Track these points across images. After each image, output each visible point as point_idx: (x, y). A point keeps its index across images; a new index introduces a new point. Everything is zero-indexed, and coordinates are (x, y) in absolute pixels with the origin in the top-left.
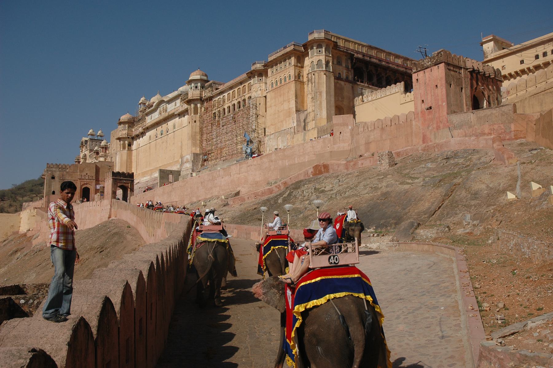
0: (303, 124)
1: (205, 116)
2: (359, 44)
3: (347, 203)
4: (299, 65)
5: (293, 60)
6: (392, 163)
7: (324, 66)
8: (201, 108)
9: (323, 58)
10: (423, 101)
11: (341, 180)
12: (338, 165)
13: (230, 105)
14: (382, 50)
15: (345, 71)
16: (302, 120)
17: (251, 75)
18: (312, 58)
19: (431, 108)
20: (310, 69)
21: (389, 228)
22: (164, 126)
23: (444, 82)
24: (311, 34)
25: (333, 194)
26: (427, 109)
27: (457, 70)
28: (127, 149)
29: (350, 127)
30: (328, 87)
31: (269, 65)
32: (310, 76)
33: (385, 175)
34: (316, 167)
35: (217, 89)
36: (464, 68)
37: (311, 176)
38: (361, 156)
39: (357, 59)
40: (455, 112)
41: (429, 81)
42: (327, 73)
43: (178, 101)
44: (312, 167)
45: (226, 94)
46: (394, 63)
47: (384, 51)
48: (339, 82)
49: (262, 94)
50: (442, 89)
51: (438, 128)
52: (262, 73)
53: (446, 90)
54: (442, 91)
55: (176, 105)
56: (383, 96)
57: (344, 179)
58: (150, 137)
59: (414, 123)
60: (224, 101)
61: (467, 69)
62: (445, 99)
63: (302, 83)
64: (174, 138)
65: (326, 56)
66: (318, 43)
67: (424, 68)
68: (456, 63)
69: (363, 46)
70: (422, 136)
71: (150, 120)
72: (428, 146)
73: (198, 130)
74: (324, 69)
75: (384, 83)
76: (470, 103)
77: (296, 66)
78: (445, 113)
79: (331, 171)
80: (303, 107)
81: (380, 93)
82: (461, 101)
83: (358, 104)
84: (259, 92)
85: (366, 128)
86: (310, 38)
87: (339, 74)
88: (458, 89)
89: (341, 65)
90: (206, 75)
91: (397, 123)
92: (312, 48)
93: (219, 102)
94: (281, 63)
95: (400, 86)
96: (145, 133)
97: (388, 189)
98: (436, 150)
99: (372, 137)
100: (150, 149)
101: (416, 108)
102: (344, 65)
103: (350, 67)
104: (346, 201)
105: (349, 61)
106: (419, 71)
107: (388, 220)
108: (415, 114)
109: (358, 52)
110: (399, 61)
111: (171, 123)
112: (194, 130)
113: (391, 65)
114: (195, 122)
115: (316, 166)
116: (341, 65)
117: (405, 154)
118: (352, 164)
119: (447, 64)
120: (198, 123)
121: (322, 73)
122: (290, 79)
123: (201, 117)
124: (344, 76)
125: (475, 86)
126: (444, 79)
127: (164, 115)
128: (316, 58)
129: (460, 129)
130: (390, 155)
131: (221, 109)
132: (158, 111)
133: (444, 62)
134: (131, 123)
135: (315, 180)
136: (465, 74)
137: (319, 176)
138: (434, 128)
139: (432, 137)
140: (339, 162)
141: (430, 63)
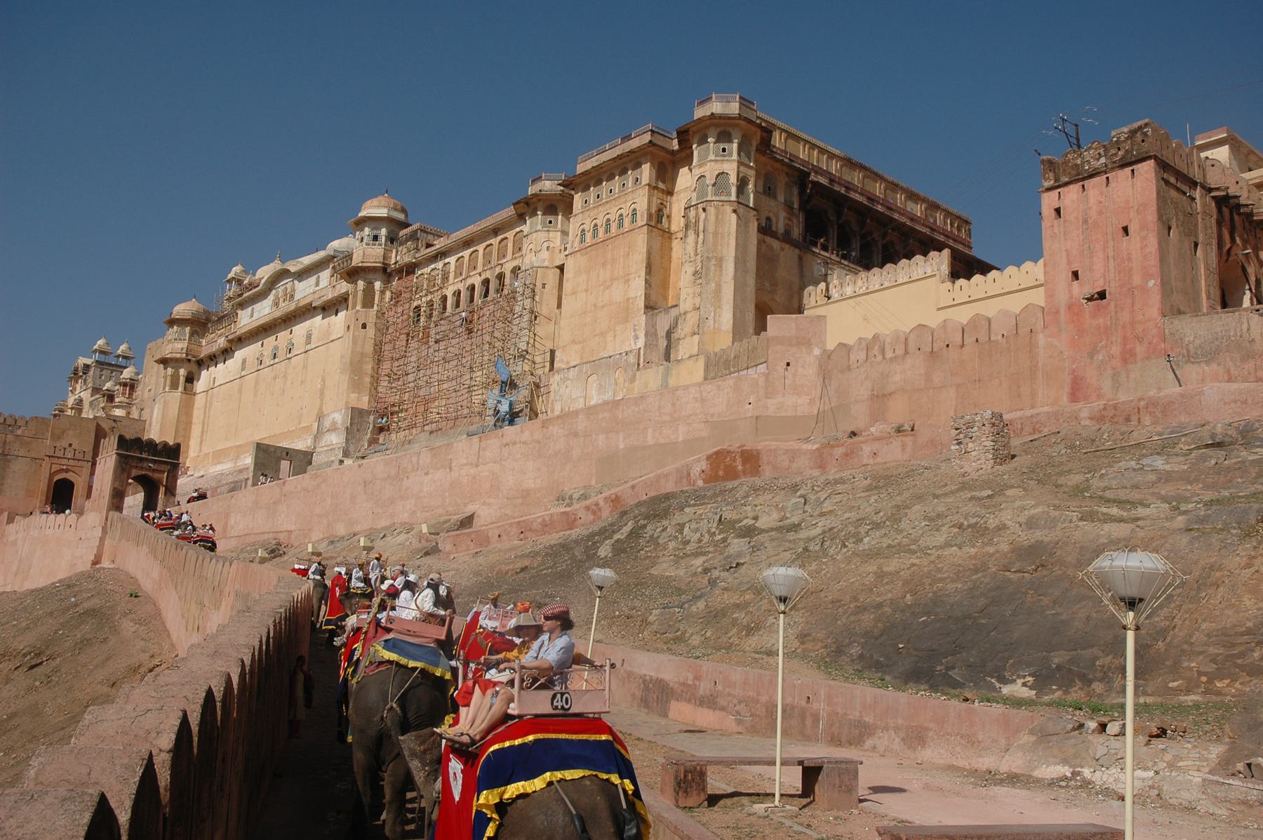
0: (663, 343)
1: (392, 313)
2: (822, 151)
3: (880, 575)
4: (661, 185)
6: (1004, 456)
7: (734, 190)
8: (383, 292)
10: (1075, 275)
11: (812, 497)
12: (793, 455)
13: (461, 286)
14: (877, 174)
15: (783, 215)
16: (662, 333)
17: (527, 207)
18: (700, 166)
19: (1102, 295)
20: (694, 195)
21: (1098, 687)
22: (283, 335)
23: (1151, 216)
24: (701, 103)
25: (809, 540)
26: (1090, 299)
27: (1185, 188)
28: (181, 389)
29: (817, 352)
30: (741, 247)
32: (692, 213)
33: (1000, 489)
34: (717, 458)
35: (429, 246)
36: (1203, 187)
37: (700, 483)
38: (853, 434)
39: (816, 184)
40: (1180, 312)
41: (1100, 213)
42: (741, 210)
43: (325, 275)
44: (703, 455)
45: (452, 260)
46: (903, 212)
47: (882, 178)
48: (768, 239)
49: (552, 259)
50: (1145, 238)
51: (1128, 357)
52: (557, 206)
53: (1160, 243)
54: (1144, 245)
55: (317, 284)
56: (886, 284)
57: (823, 495)
58: (244, 361)
59: (1041, 339)
60: (445, 278)
61: (1210, 190)
62: (1155, 270)
63: (668, 235)
64: (305, 367)
65: (740, 163)
66: (722, 128)
67: (1082, 177)
68: (1181, 166)
69: (832, 156)
70: (1067, 379)
71: (247, 319)
72: (1115, 407)
73: (369, 348)
74: (733, 198)
75: (877, 257)
76: (1216, 293)
78: (1154, 311)
79: (767, 472)
80: (666, 298)
81: (877, 277)
82: (1195, 281)
83: (813, 303)
84: (545, 254)
85: (876, 350)
86: (700, 113)
87: (768, 219)
88: (1188, 245)
89: (775, 197)
90: (403, 211)
91: (983, 338)
92: (703, 141)
93: (431, 280)
94: (611, 177)
95: (940, 262)
96: (233, 352)
97: (1038, 535)
98: (1147, 420)
99: (897, 378)
100: (240, 391)
101: (1050, 296)
102: (781, 198)
103: (796, 206)
104: (872, 568)
105: (795, 191)
106: (1066, 184)
107: (1088, 653)
108: (1049, 313)
109: (819, 171)
110: (918, 209)
111: (300, 329)
112: (359, 349)
113: (896, 216)
115: (717, 453)
116: (775, 197)
117: (1028, 429)
118: (838, 452)
119: (1163, 166)
120: (371, 331)
121: (728, 209)
122: (633, 221)
123: (380, 314)
124: (780, 227)
125: (1228, 246)
126: (1154, 208)
127: (286, 307)
128: (716, 164)
129: (1208, 363)
130: (999, 426)
131: (436, 298)
132: (271, 297)
133: (1155, 158)
134: (200, 324)
135: (715, 496)
136: (1204, 205)
137: (730, 485)
138: (1111, 357)
139: (1107, 385)
140: (795, 445)
141: (1103, 160)
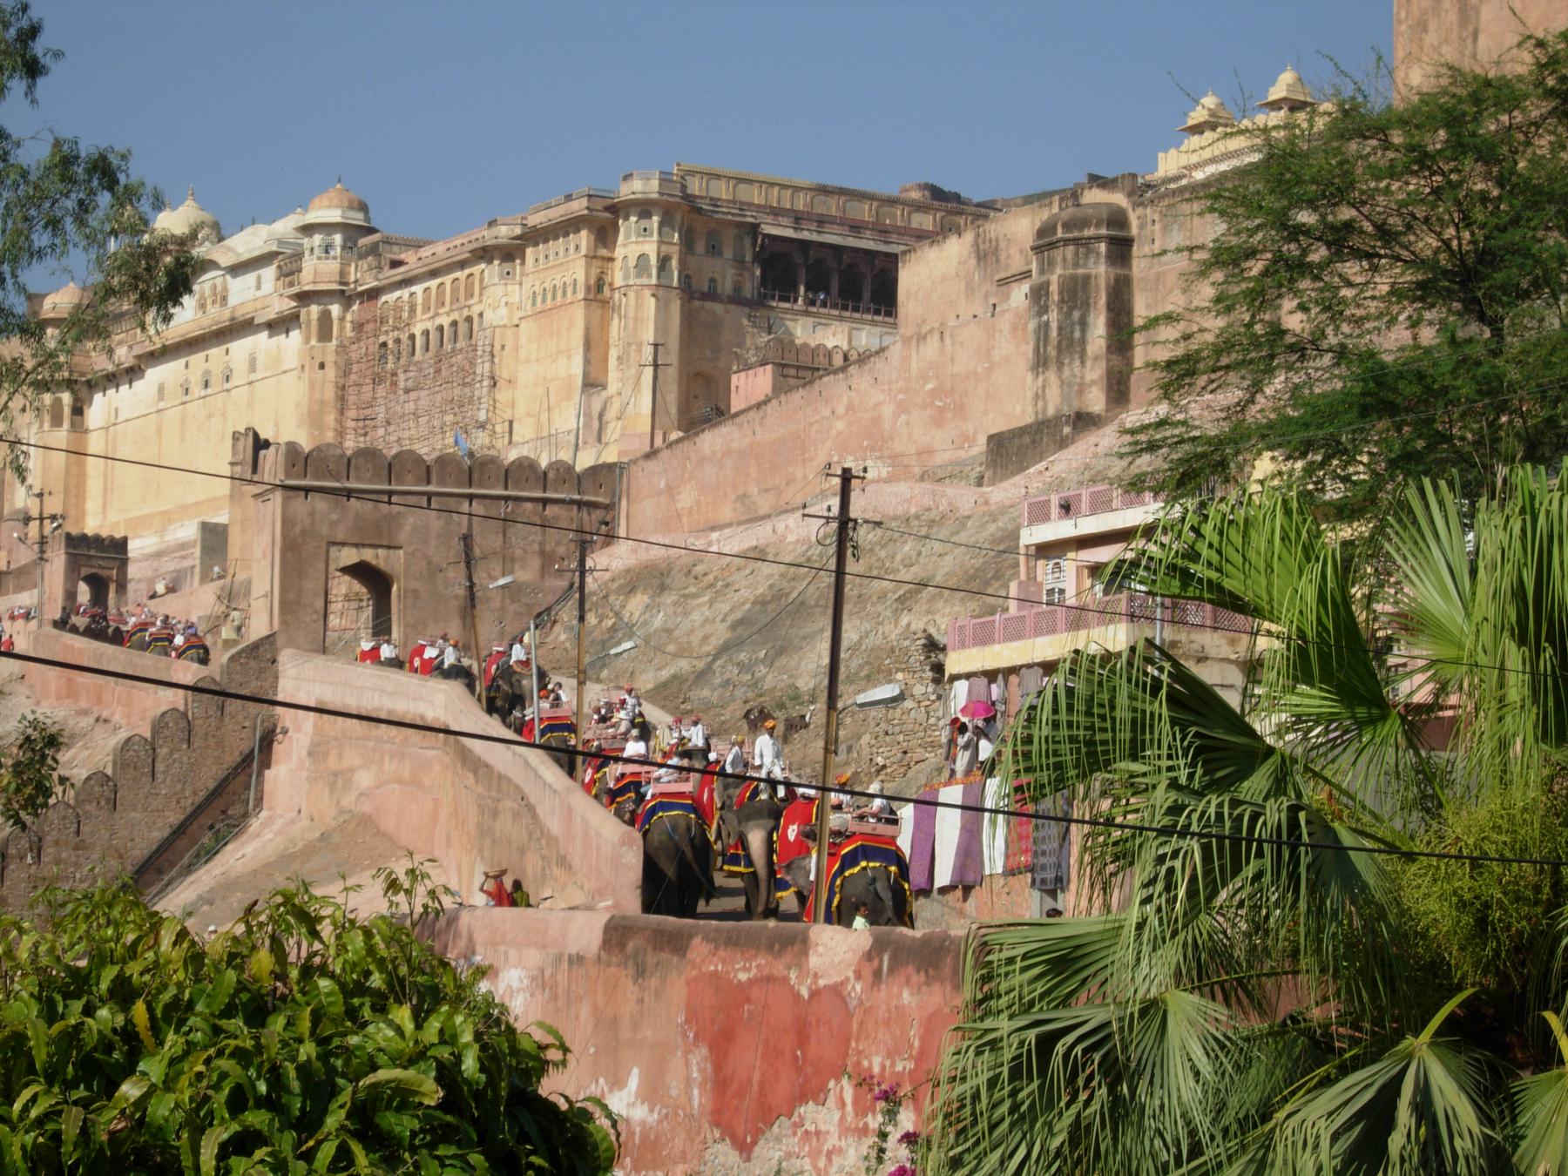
0: (596, 424)
1: (354, 347)
5: (584, 238)
7: (654, 272)
8: (342, 319)
9: (651, 248)
13: (429, 325)
15: (731, 272)
16: (595, 415)
17: (484, 254)
22: (215, 352)
28: (66, 424)
31: (536, 236)
35: (395, 264)
42: (661, 292)
43: (269, 273)
45: (418, 289)
49: (510, 318)
55: (258, 287)
58: (161, 389)
60: (413, 310)
64: (251, 404)
65: (660, 242)
66: (644, 208)
69: (797, 189)
73: (330, 393)
74: (654, 281)
77: (591, 257)
84: (503, 311)
87: (713, 280)
89: (720, 254)
90: (363, 207)
92: (626, 218)
93: (397, 308)
94: (556, 238)
96: (143, 372)
100: (159, 431)
103: (748, 258)
111: (240, 348)
112: (317, 396)
114: (322, 366)
120: (331, 373)
121: (647, 293)
122: (574, 292)
123: (342, 347)
124: (726, 287)
127: (217, 316)
128: (638, 244)
131: (404, 337)
